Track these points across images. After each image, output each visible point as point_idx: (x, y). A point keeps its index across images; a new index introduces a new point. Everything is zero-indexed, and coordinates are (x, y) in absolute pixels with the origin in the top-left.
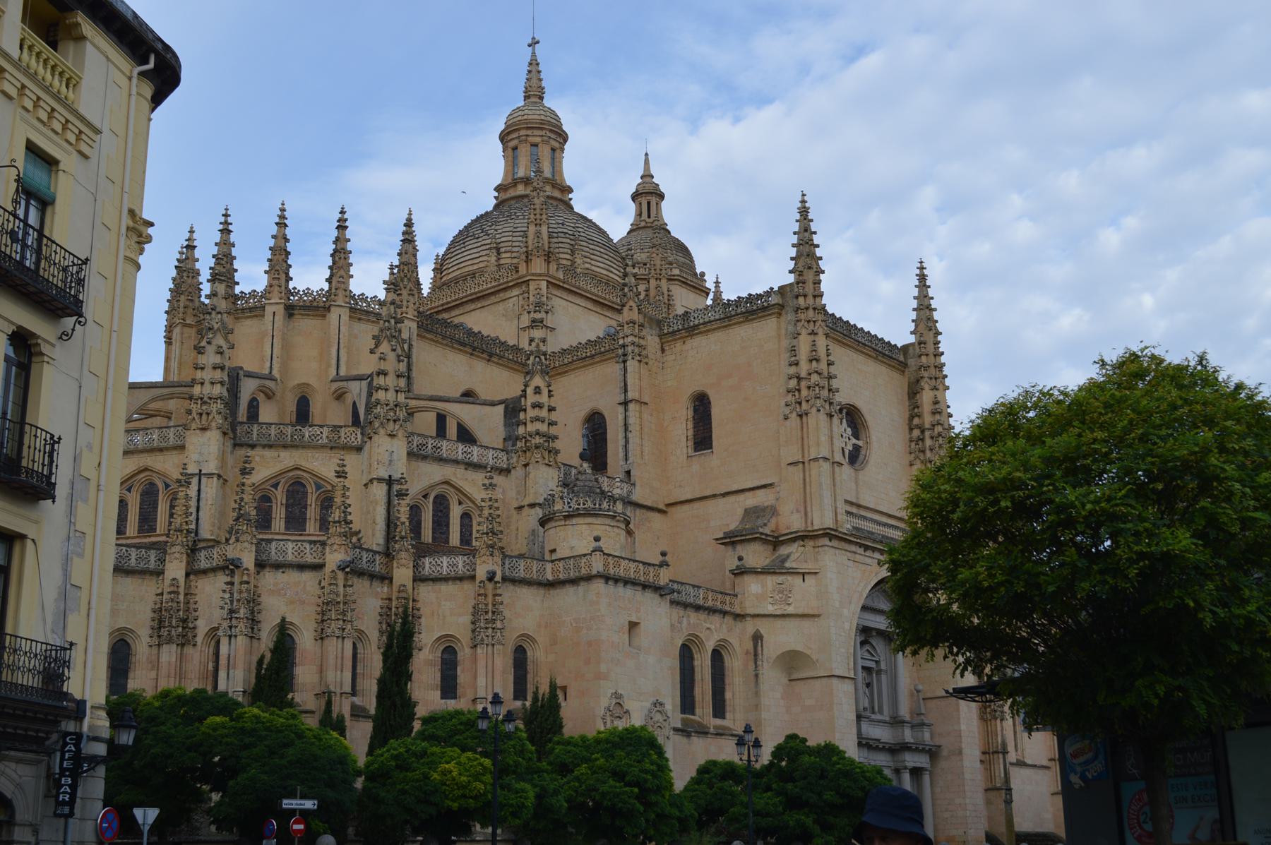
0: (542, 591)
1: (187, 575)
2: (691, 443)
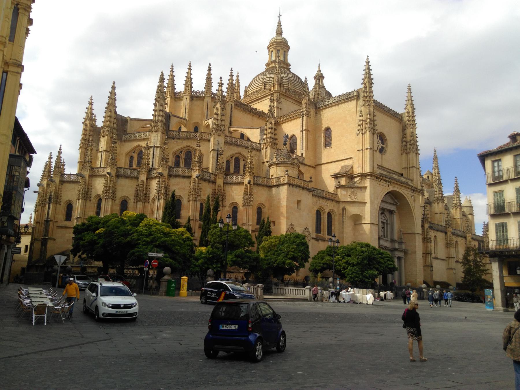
0: (267, 189)
1: (147, 179)
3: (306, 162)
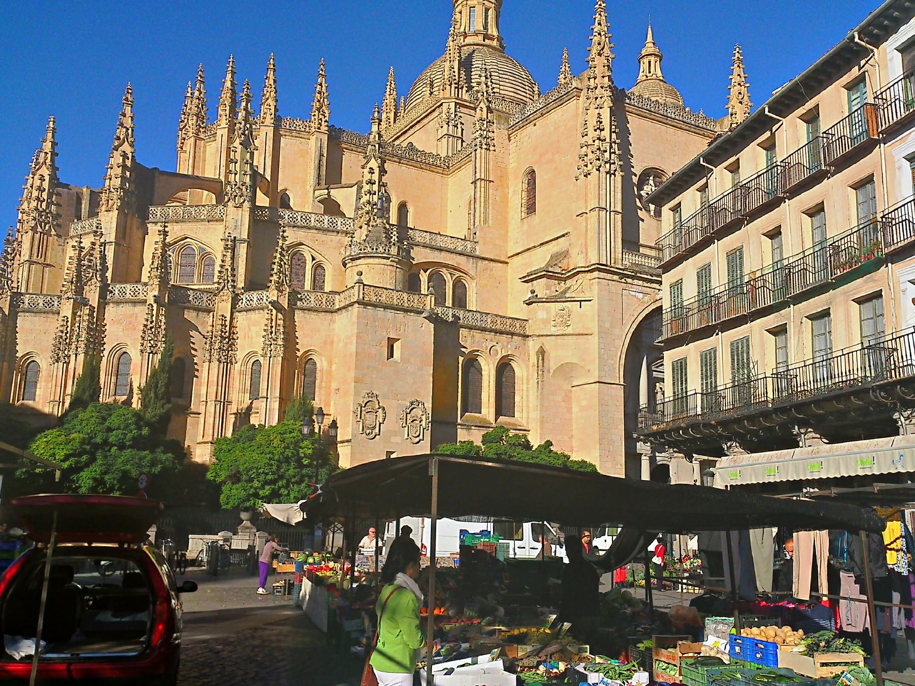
0: (329, 316)
2: (523, 209)
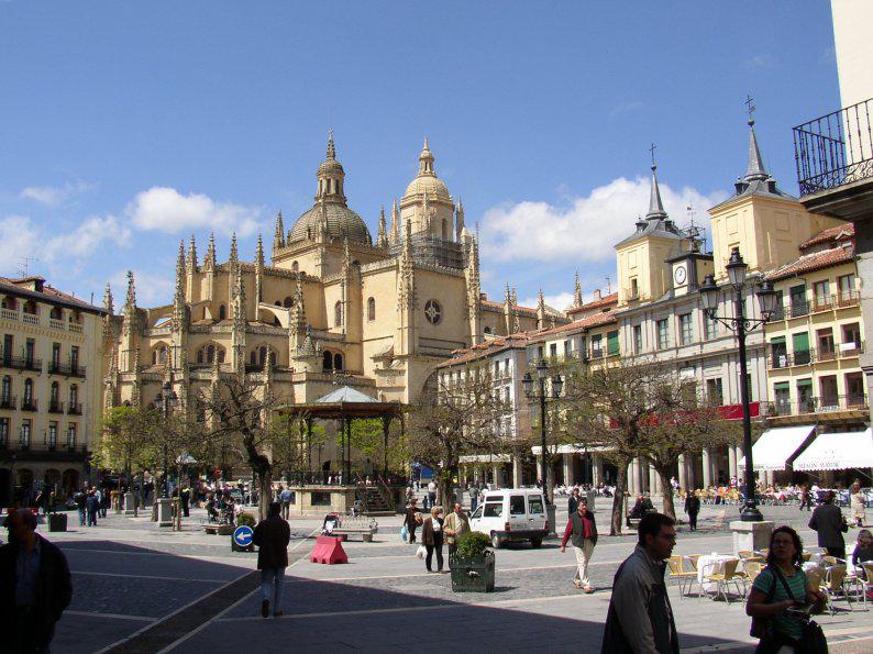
3: (348, 340)
